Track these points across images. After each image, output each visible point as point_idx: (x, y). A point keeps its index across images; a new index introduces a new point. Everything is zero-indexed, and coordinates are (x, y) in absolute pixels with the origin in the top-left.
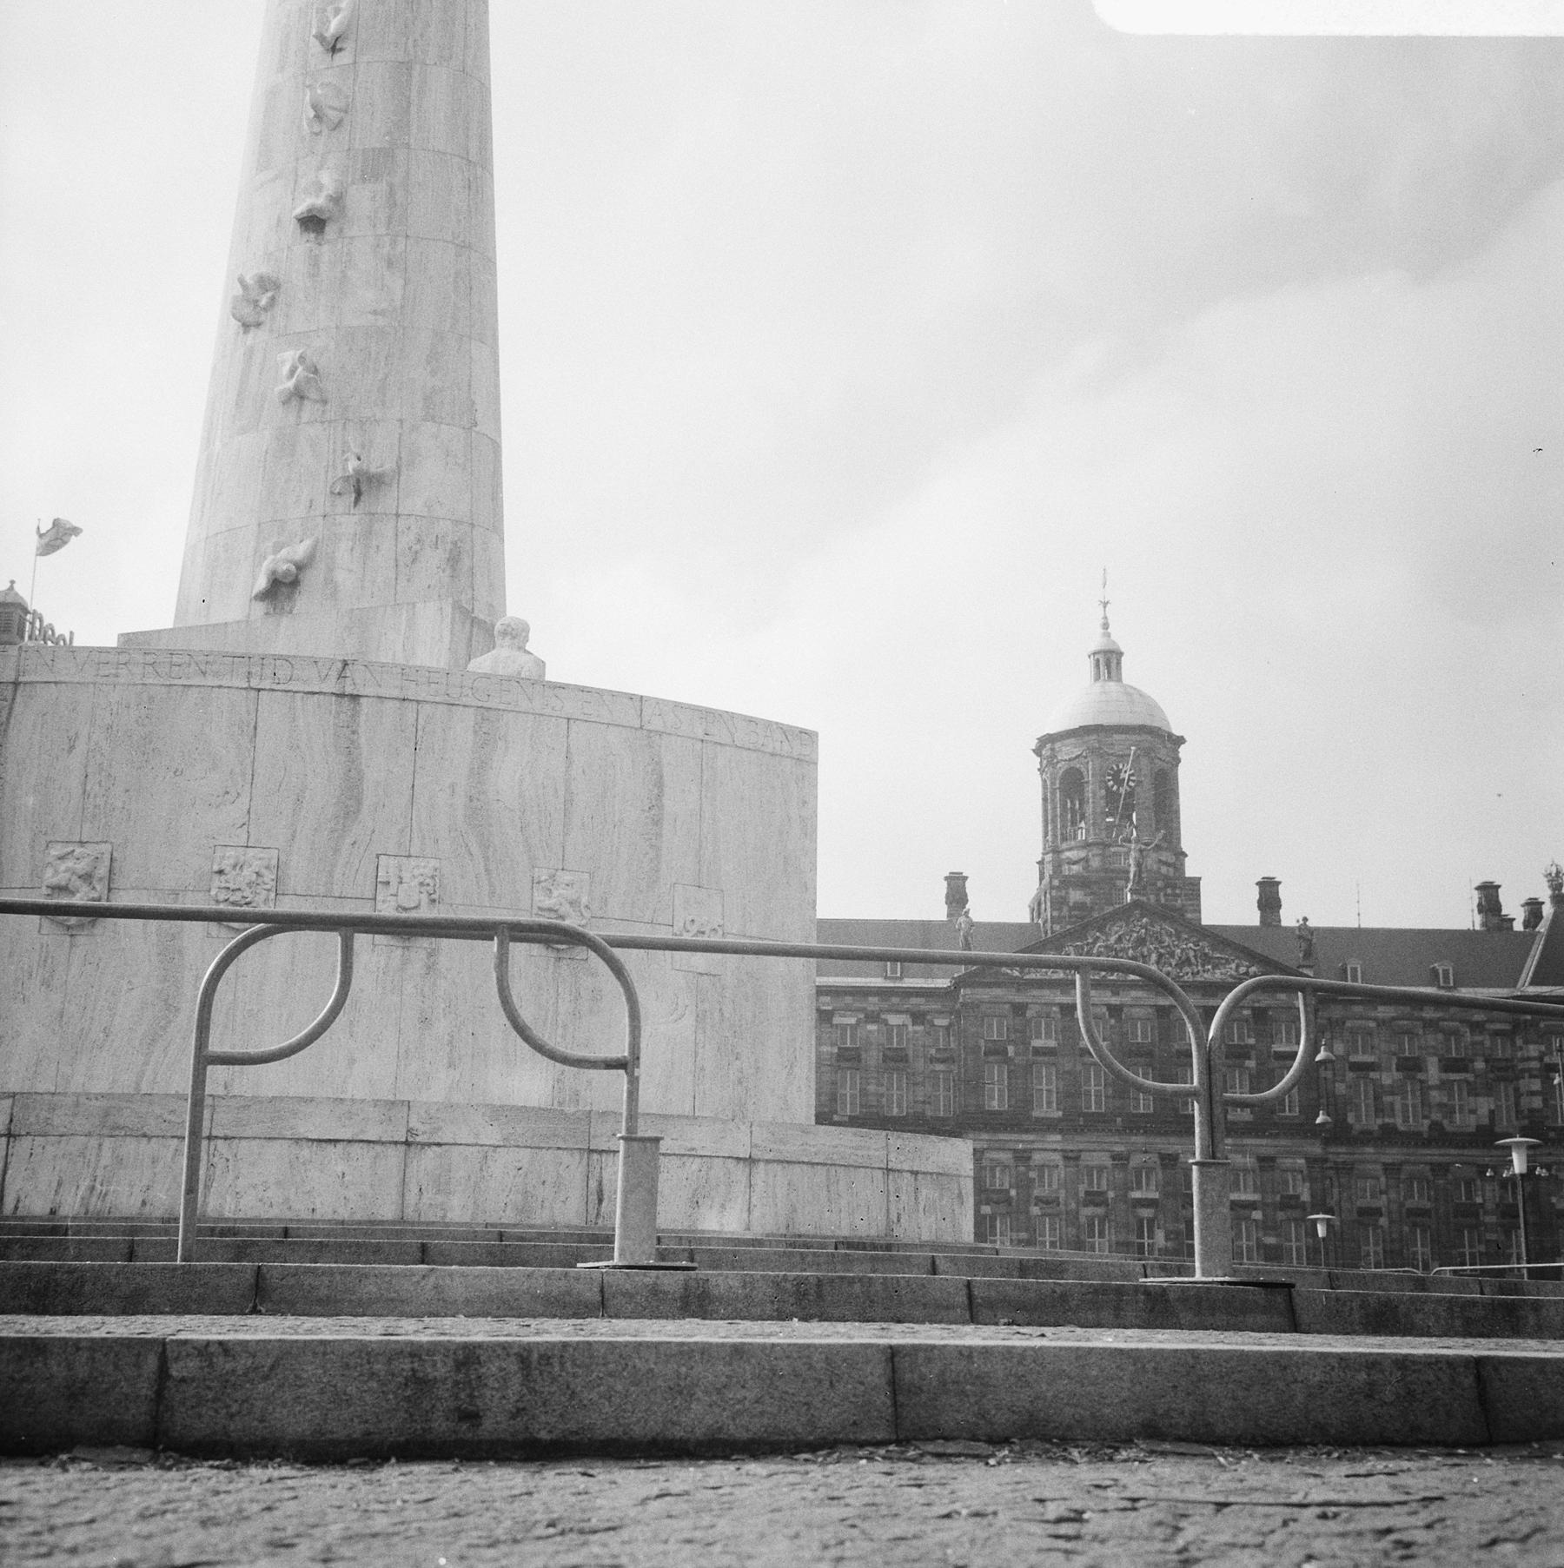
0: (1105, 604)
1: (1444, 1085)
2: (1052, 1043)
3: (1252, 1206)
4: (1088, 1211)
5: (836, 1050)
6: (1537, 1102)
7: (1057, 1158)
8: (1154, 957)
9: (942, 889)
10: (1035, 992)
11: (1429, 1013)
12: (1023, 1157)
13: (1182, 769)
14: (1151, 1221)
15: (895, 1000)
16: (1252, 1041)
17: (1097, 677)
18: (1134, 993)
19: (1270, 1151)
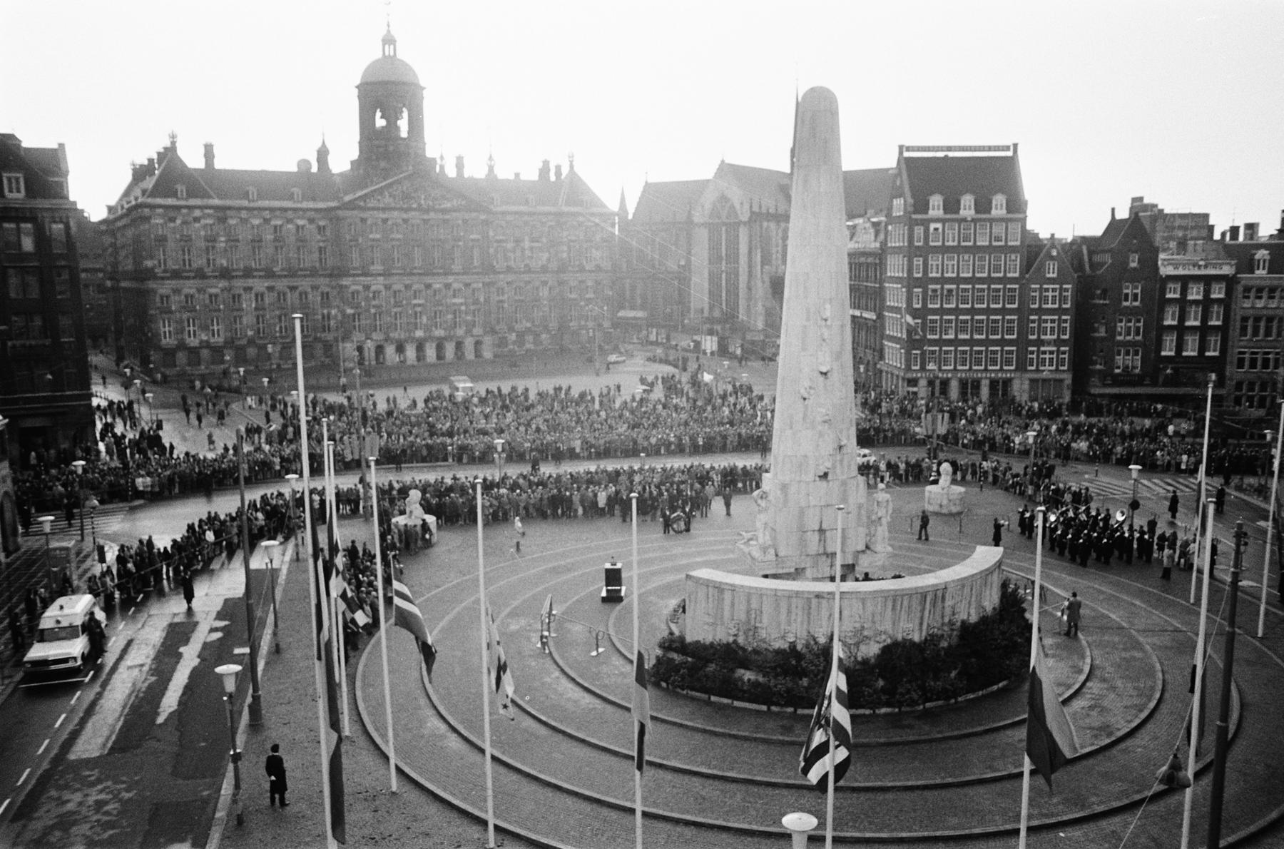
1: (531, 249)
2: (378, 236)
6: (565, 255)
7: (382, 288)
12: (367, 288)
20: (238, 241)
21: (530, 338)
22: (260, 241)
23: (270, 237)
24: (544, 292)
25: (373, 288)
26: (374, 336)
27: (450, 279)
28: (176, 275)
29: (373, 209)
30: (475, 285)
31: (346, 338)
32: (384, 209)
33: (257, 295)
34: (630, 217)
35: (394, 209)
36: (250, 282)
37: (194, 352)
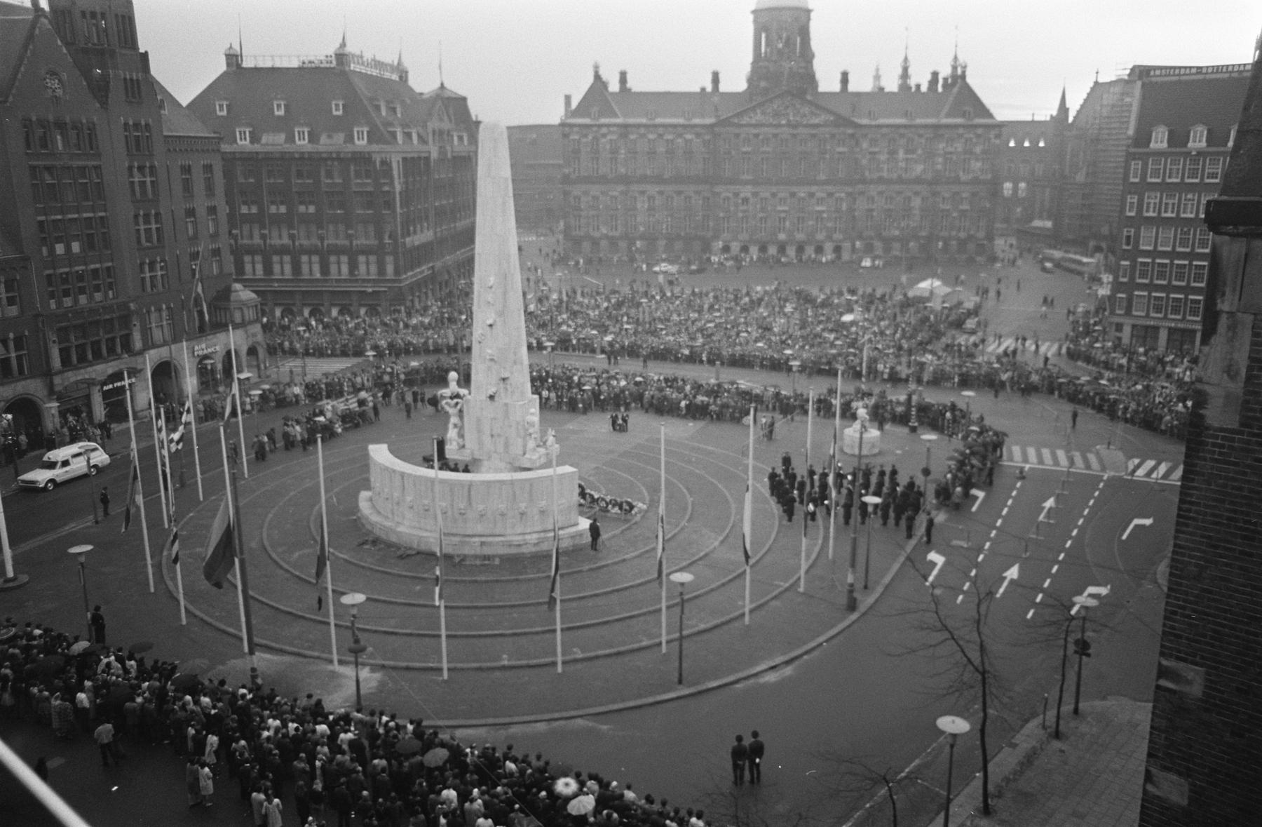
2: (749, 149)
6: (939, 167)
7: (749, 195)
11: (902, 131)
21: (897, 245)
22: (655, 153)
23: (662, 149)
24: (917, 202)
25: (742, 195)
26: (740, 237)
27: (814, 189)
28: (588, 180)
31: (716, 237)
32: (755, 126)
33: (649, 198)
34: (1071, 120)
35: (762, 125)
37: (595, 243)
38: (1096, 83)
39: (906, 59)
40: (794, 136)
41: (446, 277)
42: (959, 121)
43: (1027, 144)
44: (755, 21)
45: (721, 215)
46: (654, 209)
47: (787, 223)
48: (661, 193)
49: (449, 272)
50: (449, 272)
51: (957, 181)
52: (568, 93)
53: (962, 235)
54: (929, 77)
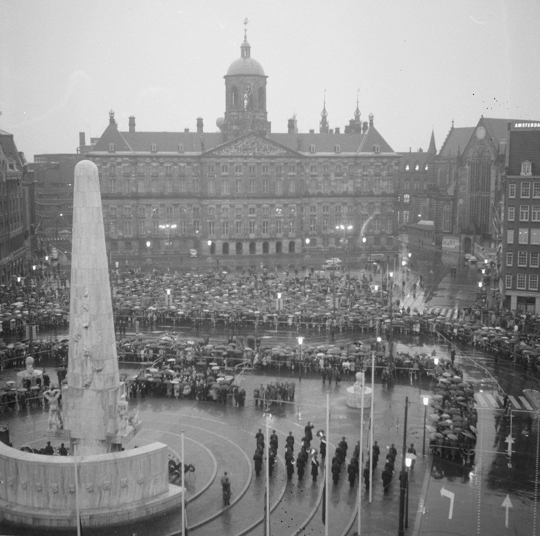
0: (246, 31)
1: (336, 180)
2: (226, 174)
3: (281, 218)
4: (237, 220)
5: (165, 174)
6: (359, 185)
7: (228, 206)
8: (257, 148)
9: (196, 122)
10: (223, 159)
11: (333, 160)
12: (219, 206)
13: (268, 87)
14: (254, 223)
15: (182, 159)
16: (283, 172)
17: (243, 55)
18: (250, 159)
19: (287, 203)
20: (143, 176)
21: (333, 240)
22: (157, 176)
24: (345, 210)
27: (274, 201)
29: (224, 157)
30: (290, 206)
32: (231, 157)
34: (438, 153)
35: (237, 157)
36: (150, 201)
38: (453, 129)
39: (324, 110)
40: (258, 164)
41: (3, 274)
42: (370, 154)
43: (417, 168)
44: (227, 84)
45: (208, 221)
46: (158, 218)
47: (256, 226)
48: (163, 205)
49: (4, 269)
50: (4, 269)
51: (371, 195)
52: (82, 131)
53: (377, 232)
54: (348, 124)
